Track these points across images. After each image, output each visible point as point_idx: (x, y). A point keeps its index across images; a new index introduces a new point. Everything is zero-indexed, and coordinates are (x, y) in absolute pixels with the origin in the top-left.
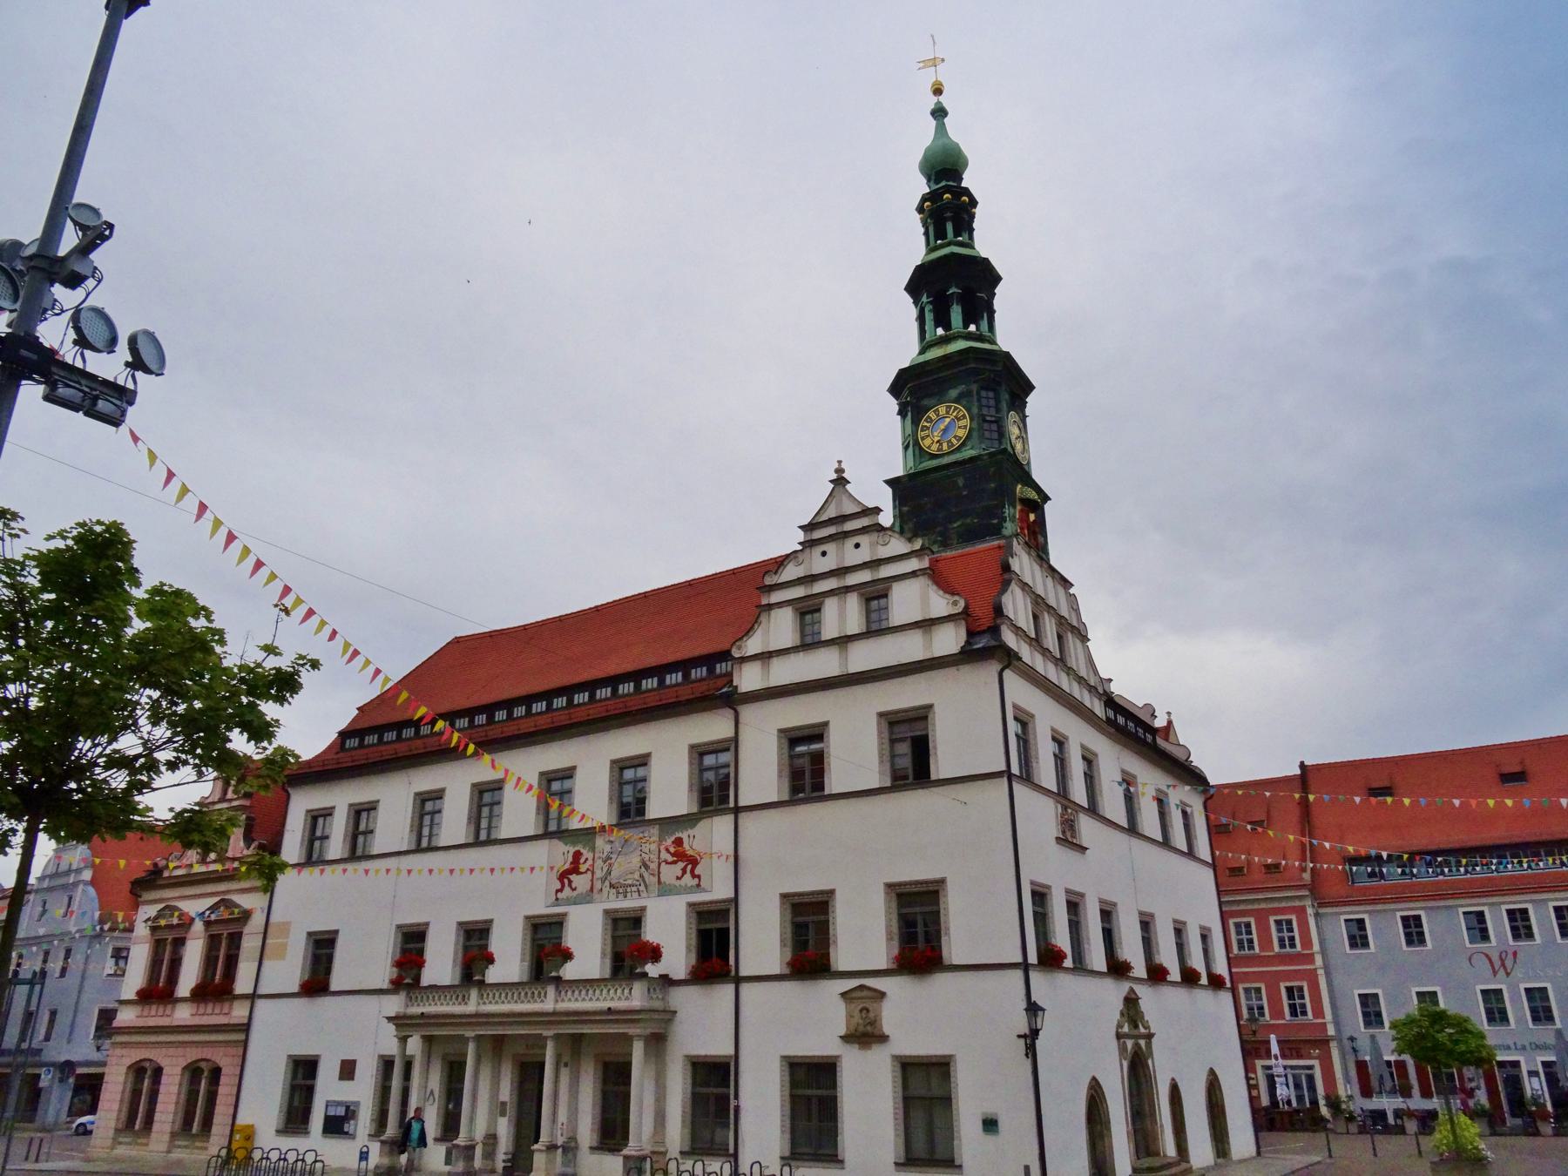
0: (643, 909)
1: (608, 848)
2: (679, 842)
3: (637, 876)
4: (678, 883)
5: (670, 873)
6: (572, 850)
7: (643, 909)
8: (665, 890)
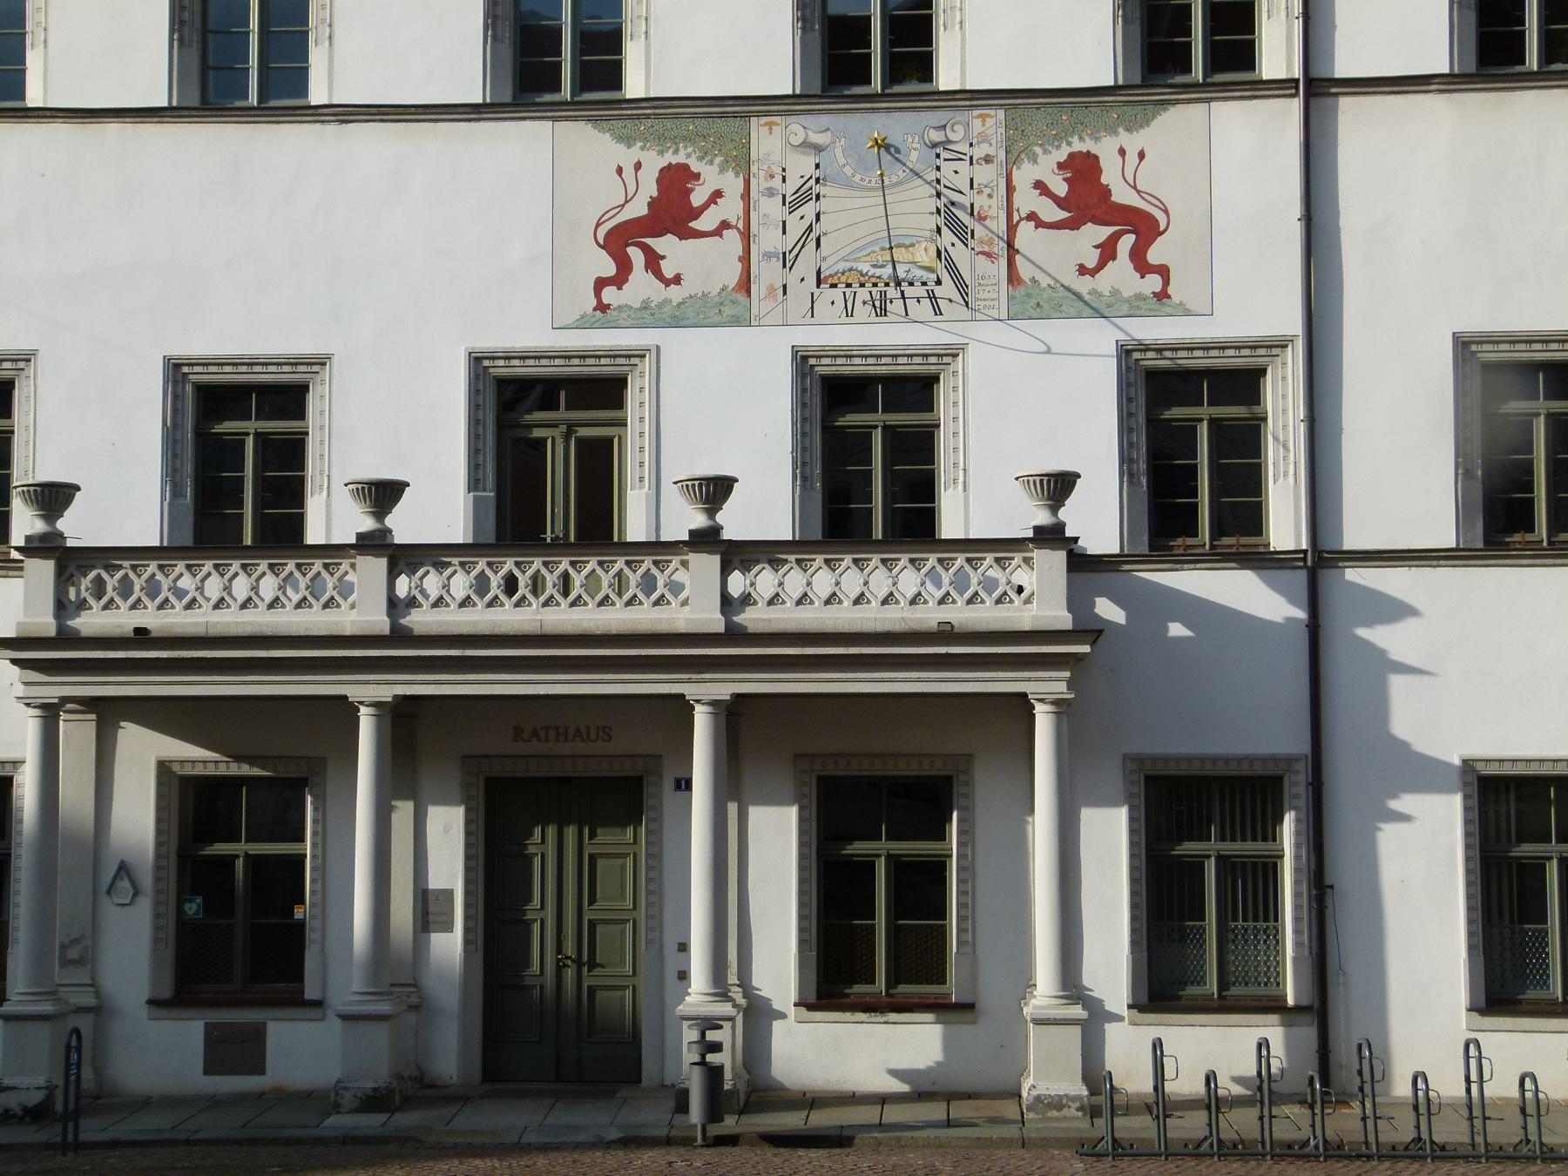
0: (953, 353)
1: (802, 166)
2: (1083, 169)
3: (924, 255)
4: (1084, 285)
5: (1057, 253)
6: (655, 162)
7: (953, 353)
8: (1028, 299)
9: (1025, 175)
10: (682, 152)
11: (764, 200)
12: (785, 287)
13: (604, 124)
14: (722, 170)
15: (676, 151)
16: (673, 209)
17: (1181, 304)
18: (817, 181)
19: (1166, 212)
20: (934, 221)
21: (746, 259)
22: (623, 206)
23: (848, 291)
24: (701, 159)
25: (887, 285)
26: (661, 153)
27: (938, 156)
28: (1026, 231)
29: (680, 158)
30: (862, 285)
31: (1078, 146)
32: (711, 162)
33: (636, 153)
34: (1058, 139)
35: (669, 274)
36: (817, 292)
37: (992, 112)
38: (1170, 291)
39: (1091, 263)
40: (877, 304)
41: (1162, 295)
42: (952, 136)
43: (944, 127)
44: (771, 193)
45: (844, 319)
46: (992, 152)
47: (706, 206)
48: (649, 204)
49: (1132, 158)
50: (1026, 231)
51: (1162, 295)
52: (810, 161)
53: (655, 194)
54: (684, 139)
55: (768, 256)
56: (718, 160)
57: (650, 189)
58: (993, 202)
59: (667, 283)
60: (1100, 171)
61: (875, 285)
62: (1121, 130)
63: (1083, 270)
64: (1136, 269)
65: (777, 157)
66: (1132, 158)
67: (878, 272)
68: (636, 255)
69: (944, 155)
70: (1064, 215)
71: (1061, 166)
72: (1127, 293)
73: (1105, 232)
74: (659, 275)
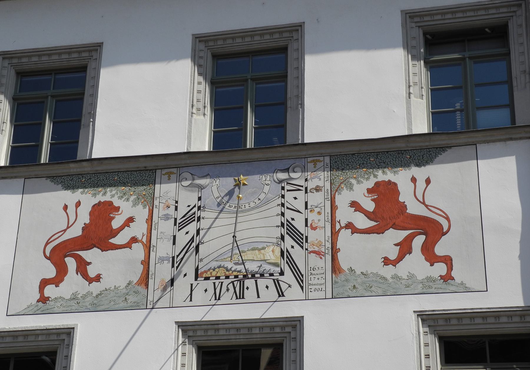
2: (386, 193)
3: (272, 254)
4: (389, 271)
10: (109, 194)
14: (135, 204)
15: (105, 194)
17: (462, 283)
18: (199, 208)
19: (448, 219)
20: (278, 232)
21: (146, 263)
22: (65, 231)
23: (217, 282)
24: (121, 198)
26: (94, 195)
27: (283, 188)
28: (345, 235)
29: (107, 198)
30: (227, 277)
32: (128, 200)
38: (453, 274)
41: (447, 278)
44: (167, 217)
46: (321, 184)
47: (121, 228)
48: (83, 229)
49: (421, 184)
50: (345, 235)
51: (447, 278)
52: (195, 196)
55: (162, 260)
56: (132, 198)
57: (84, 218)
58: (322, 217)
60: (398, 193)
63: (387, 261)
64: (426, 260)
66: (421, 184)
68: (71, 263)
69: (287, 187)
70: (373, 224)
72: (420, 277)
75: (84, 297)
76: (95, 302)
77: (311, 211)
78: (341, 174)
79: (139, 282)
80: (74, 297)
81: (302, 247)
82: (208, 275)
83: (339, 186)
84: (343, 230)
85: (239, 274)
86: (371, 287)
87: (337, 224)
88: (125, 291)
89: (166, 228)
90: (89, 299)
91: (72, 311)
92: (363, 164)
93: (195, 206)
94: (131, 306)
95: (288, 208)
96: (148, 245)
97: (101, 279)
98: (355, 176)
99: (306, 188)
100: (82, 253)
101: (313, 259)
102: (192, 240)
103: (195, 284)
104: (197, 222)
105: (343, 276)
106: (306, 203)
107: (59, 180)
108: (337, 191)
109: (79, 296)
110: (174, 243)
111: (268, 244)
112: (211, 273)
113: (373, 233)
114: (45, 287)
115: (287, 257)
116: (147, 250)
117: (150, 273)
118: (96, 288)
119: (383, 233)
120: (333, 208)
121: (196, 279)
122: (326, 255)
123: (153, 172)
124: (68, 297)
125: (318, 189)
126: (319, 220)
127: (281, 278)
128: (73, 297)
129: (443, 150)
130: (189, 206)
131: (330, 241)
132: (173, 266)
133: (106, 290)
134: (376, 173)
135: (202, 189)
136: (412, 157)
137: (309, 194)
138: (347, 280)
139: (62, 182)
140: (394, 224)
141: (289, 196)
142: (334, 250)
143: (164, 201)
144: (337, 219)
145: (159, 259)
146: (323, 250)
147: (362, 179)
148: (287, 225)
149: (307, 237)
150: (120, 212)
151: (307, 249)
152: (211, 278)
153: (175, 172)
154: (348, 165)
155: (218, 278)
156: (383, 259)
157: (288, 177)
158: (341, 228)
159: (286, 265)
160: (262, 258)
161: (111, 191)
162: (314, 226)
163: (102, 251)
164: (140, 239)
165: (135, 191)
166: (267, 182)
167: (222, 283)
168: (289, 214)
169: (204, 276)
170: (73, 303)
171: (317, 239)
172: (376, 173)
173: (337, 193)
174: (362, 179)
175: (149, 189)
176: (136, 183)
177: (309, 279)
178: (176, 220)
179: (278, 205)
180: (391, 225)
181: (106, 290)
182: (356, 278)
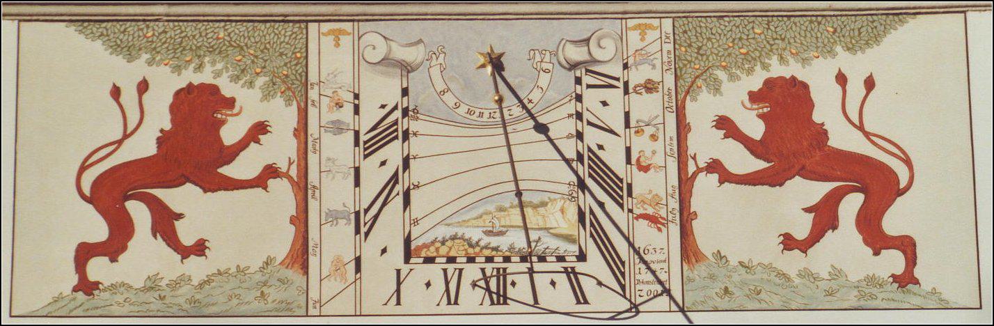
1: (382, 92)
2: (786, 101)
3: (561, 218)
5: (748, 221)
6: (167, 84)
9: (702, 110)
10: (208, 69)
11: (327, 139)
12: (358, 261)
13: (94, 27)
14: (267, 96)
15: (199, 68)
16: (195, 146)
18: (405, 112)
19: (908, 162)
21: (301, 220)
22: (119, 143)
24: (235, 79)
25: (507, 259)
26: (177, 69)
27: (578, 81)
28: (706, 184)
30: (471, 260)
31: (778, 70)
32: (251, 84)
33: (139, 68)
34: (749, 61)
35: (187, 239)
36: (405, 269)
37: (656, 22)
39: (802, 230)
40: (493, 287)
42: (598, 54)
43: (587, 41)
44: (338, 128)
45: (444, 308)
46: (656, 76)
47: (242, 145)
49: (856, 88)
50: (706, 184)
53: (167, 126)
54: (211, 50)
55: (334, 217)
56: (261, 81)
57: (159, 119)
58: (659, 145)
59: (185, 252)
60: (810, 105)
61: (489, 260)
62: (838, 49)
63: (789, 242)
65: (346, 79)
66: (856, 88)
67: (494, 241)
68: (139, 212)
69: (587, 79)
70: (761, 165)
71: (754, 97)
73: (818, 190)
74: (172, 241)
75: (175, 285)
76: (198, 297)
77: (637, 132)
78: (696, 58)
79: (288, 261)
80: (152, 285)
81: (621, 206)
82: (431, 252)
83: (693, 83)
84: (702, 175)
85: (494, 253)
86: (759, 293)
87: (691, 163)
88: (258, 277)
89: (336, 150)
90: (185, 290)
91: (151, 314)
92: (740, 39)
93: (396, 108)
94: (277, 310)
95: (589, 123)
96: (302, 185)
97: (207, 251)
98: (724, 64)
99: (626, 84)
100: (165, 195)
101: (645, 234)
102: (395, 179)
103: (405, 269)
104: (404, 142)
105: (703, 268)
106: (627, 115)
107: (95, 29)
108: (688, 92)
109: (163, 283)
110: (357, 183)
111: (553, 196)
112: (437, 250)
113: (763, 184)
114: (88, 259)
115: (592, 225)
116: (301, 194)
117: (311, 244)
118: (196, 268)
119: (781, 185)
120: (682, 128)
121: (407, 261)
122: (670, 225)
123: (300, 27)
124: (139, 283)
125: (649, 86)
126: (654, 153)
127: (580, 267)
128: (149, 284)
129: (900, 20)
130: (383, 107)
131: (677, 196)
132: (358, 231)
133: (220, 273)
134: (767, 61)
135: (408, 72)
136: (839, 30)
137: (633, 96)
138: (712, 277)
139: (102, 34)
140: (803, 168)
141: (592, 98)
142: (685, 214)
143: (329, 92)
144: (691, 152)
145: (327, 214)
146: (663, 213)
147: (738, 72)
148: (590, 158)
149: (630, 186)
150: (236, 111)
151: (630, 211)
152: (438, 260)
153: (350, 30)
154: (709, 39)
155: (451, 260)
156: (782, 238)
157: (587, 57)
158: (699, 170)
159: (590, 241)
160: (542, 225)
161: (213, 63)
162: (644, 164)
163: (205, 191)
164: (284, 170)
165: (264, 67)
166: (545, 66)
167: (461, 270)
168: (593, 137)
169: (423, 254)
170: (150, 297)
171: (651, 191)
172: (767, 61)
173: (688, 98)
174: (738, 72)
175: (296, 65)
176: (266, 48)
177: (637, 271)
178: (357, 134)
179: (570, 116)
180: (797, 167)
181: (220, 273)
182: (729, 274)
